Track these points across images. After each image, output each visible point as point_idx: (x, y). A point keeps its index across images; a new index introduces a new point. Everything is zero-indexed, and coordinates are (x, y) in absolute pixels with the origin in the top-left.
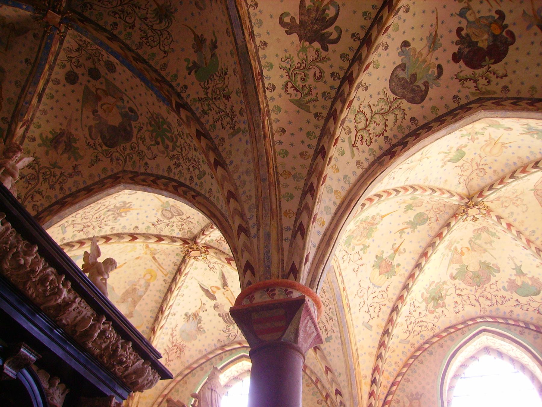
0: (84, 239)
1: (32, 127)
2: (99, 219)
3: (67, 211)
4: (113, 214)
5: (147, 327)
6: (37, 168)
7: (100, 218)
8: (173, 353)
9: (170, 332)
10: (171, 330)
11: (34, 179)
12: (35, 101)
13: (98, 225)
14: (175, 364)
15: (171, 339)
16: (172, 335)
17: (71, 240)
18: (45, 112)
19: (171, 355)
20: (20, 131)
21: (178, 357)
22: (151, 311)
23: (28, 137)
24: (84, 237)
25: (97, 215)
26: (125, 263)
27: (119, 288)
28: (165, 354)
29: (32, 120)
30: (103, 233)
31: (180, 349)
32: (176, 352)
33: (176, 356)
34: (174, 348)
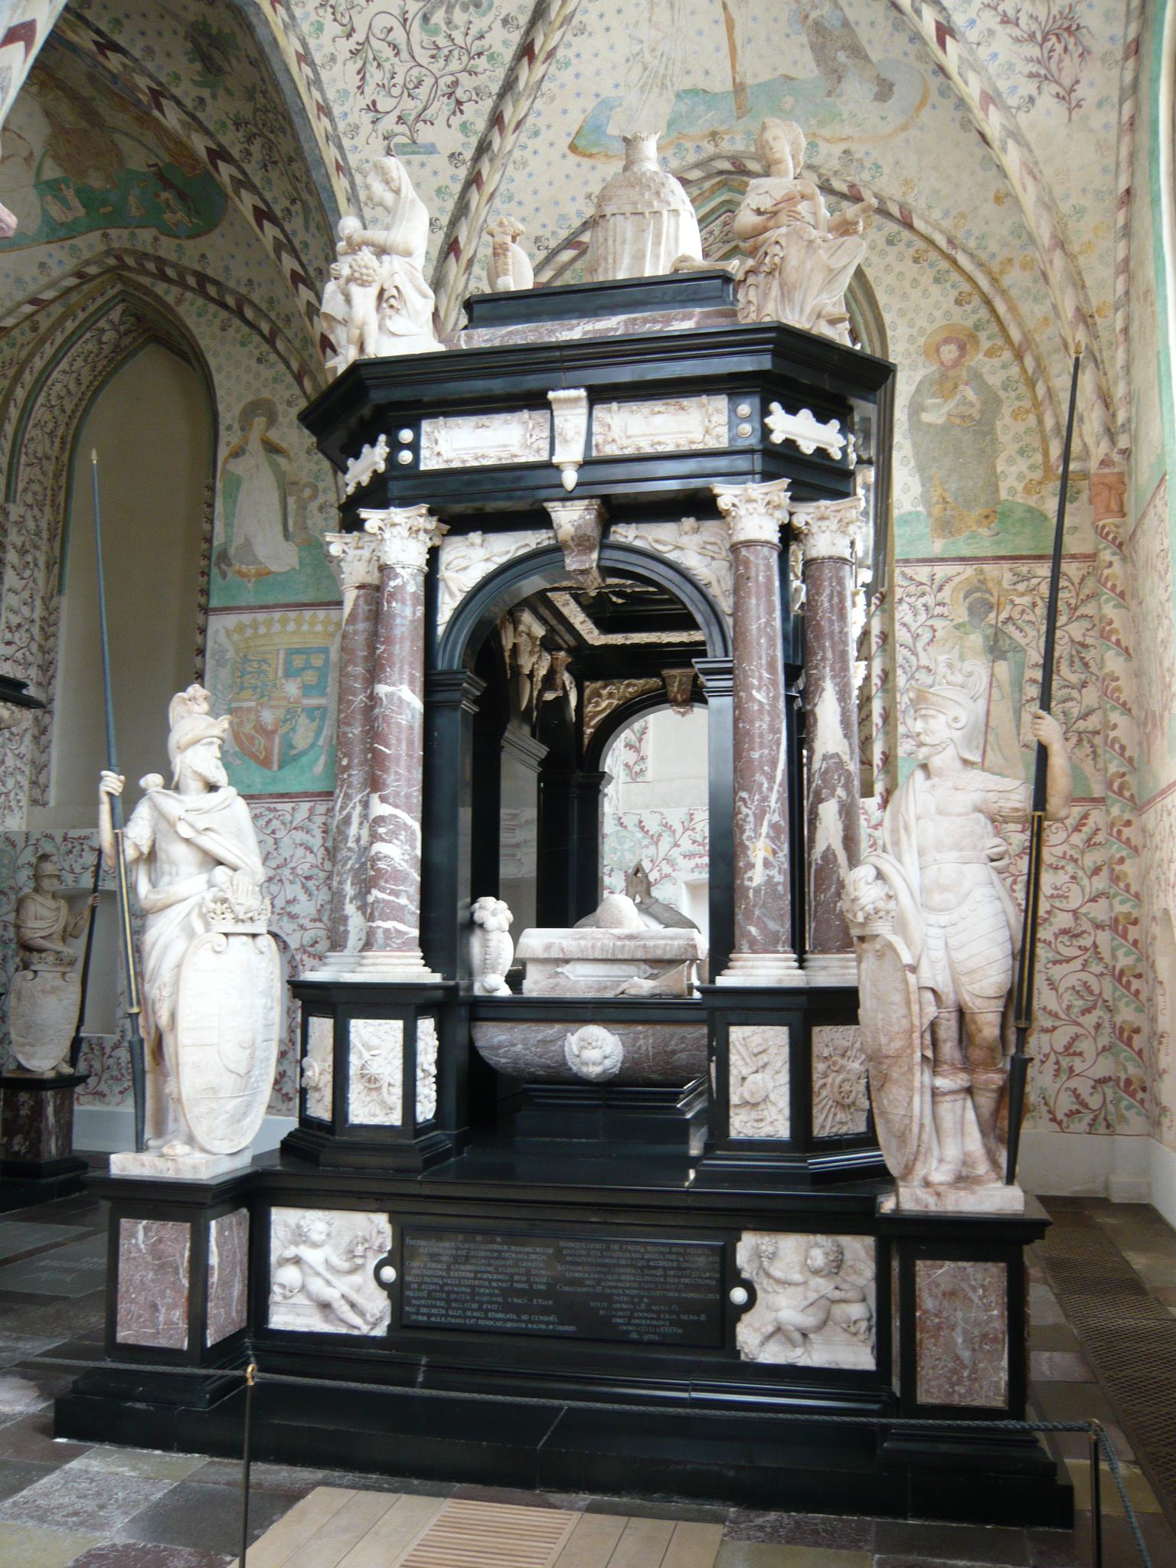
0: (496, 107)
1: (177, 91)
2: (446, 52)
3: (306, 147)
4: (450, 8)
5: (934, 73)
6: (254, 130)
7: (438, 48)
8: (1061, 61)
9: (990, 20)
10: (988, 14)
11: (270, 149)
12: (114, 62)
13: (465, 58)
14: (1092, 84)
15: (1017, 32)
16: (1005, 20)
17: (474, 141)
18: (149, 51)
19: (1060, 70)
20: (172, 118)
21: (1081, 55)
22: (896, 27)
23: (195, 108)
24: (488, 104)
25: (423, 57)
26: (725, 6)
27: (795, 63)
28: (1045, 86)
29: (160, 84)
30: (508, 55)
31: (1068, 29)
32: (1066, 49)
33: (1077, 60)
34: (1049, 45)
